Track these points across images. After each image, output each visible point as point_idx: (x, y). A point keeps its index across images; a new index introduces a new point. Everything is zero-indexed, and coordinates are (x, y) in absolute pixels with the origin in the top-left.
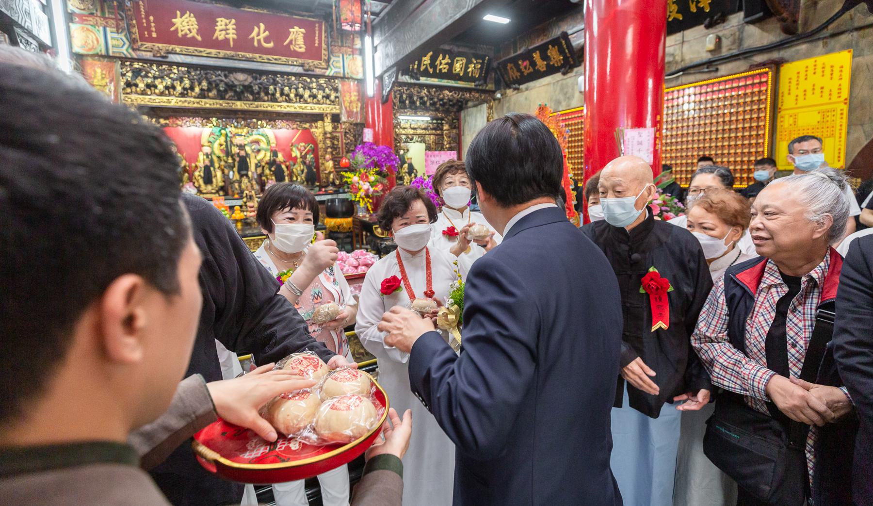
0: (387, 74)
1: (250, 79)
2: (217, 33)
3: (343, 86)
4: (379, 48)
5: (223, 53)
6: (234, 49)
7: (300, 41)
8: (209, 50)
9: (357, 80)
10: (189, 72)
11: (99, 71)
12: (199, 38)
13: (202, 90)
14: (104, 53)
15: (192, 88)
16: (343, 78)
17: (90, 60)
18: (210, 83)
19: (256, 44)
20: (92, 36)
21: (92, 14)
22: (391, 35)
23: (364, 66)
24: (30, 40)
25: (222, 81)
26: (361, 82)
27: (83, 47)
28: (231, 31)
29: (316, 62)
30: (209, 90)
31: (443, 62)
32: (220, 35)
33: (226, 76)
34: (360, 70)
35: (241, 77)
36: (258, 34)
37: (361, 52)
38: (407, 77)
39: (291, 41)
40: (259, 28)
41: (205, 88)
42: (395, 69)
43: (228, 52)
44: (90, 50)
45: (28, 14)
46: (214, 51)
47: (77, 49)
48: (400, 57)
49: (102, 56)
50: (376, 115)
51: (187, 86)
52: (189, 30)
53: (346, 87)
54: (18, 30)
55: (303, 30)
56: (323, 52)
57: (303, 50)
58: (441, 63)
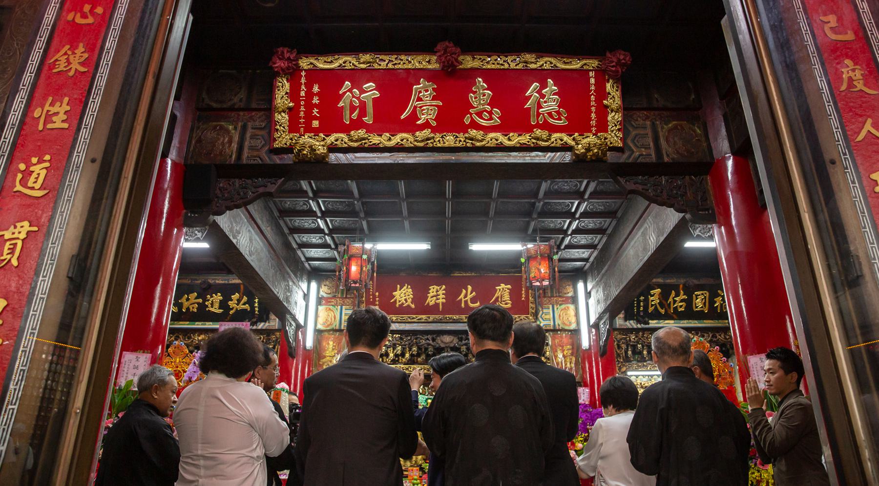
0: (602, 322)
1: (456, 340)
2: (429, 299)
3: (553, 339)
4: (593, 293)
5: (432, 317)
6: (443, 312)
7: (507, 297)
8: (420, 317)
9: (571, 331)
10: (401, 339)
11: (331, 343)
12: (413, 306)
13: (412, 355)
14: (337, 328)
15: (403, 355)
16: (555, 331)
17: (326, 333)
18: (419, 348)
19: (463, 305)
20: (331, 314)
21: (334, 297)
22: (601, 280)
23: (577, 315)
24: (293, 323)
25: (429, 344)
26: (576, 332)
27: (324, 324)
28: (441, 296)
29: (523, 317)
30: (418, 355)
31: (677, 299)
32: (431, 301)
33: (434, 340)
34: (573, 319)
35: (447, 339)
36: (466, 296)
37: (574, 300)
38: (631, 322)
39: (498, 298)
40: (467, 290)
41: (415, 353)
42: (607, 316)
43: (437, 316)
44: (328, 326)
45: (296, 303)
46: (424, 317)
47: (320, 327)
48: (608, 303)
49: (335, 331)
50: (596, 367)
51: (399, 352)
52: (406, 300)
53: (557, 341)
54: (288, 316)
55: (509, 286)
56: (531, 305)
57: (509, 306)
58: (675, 302)
